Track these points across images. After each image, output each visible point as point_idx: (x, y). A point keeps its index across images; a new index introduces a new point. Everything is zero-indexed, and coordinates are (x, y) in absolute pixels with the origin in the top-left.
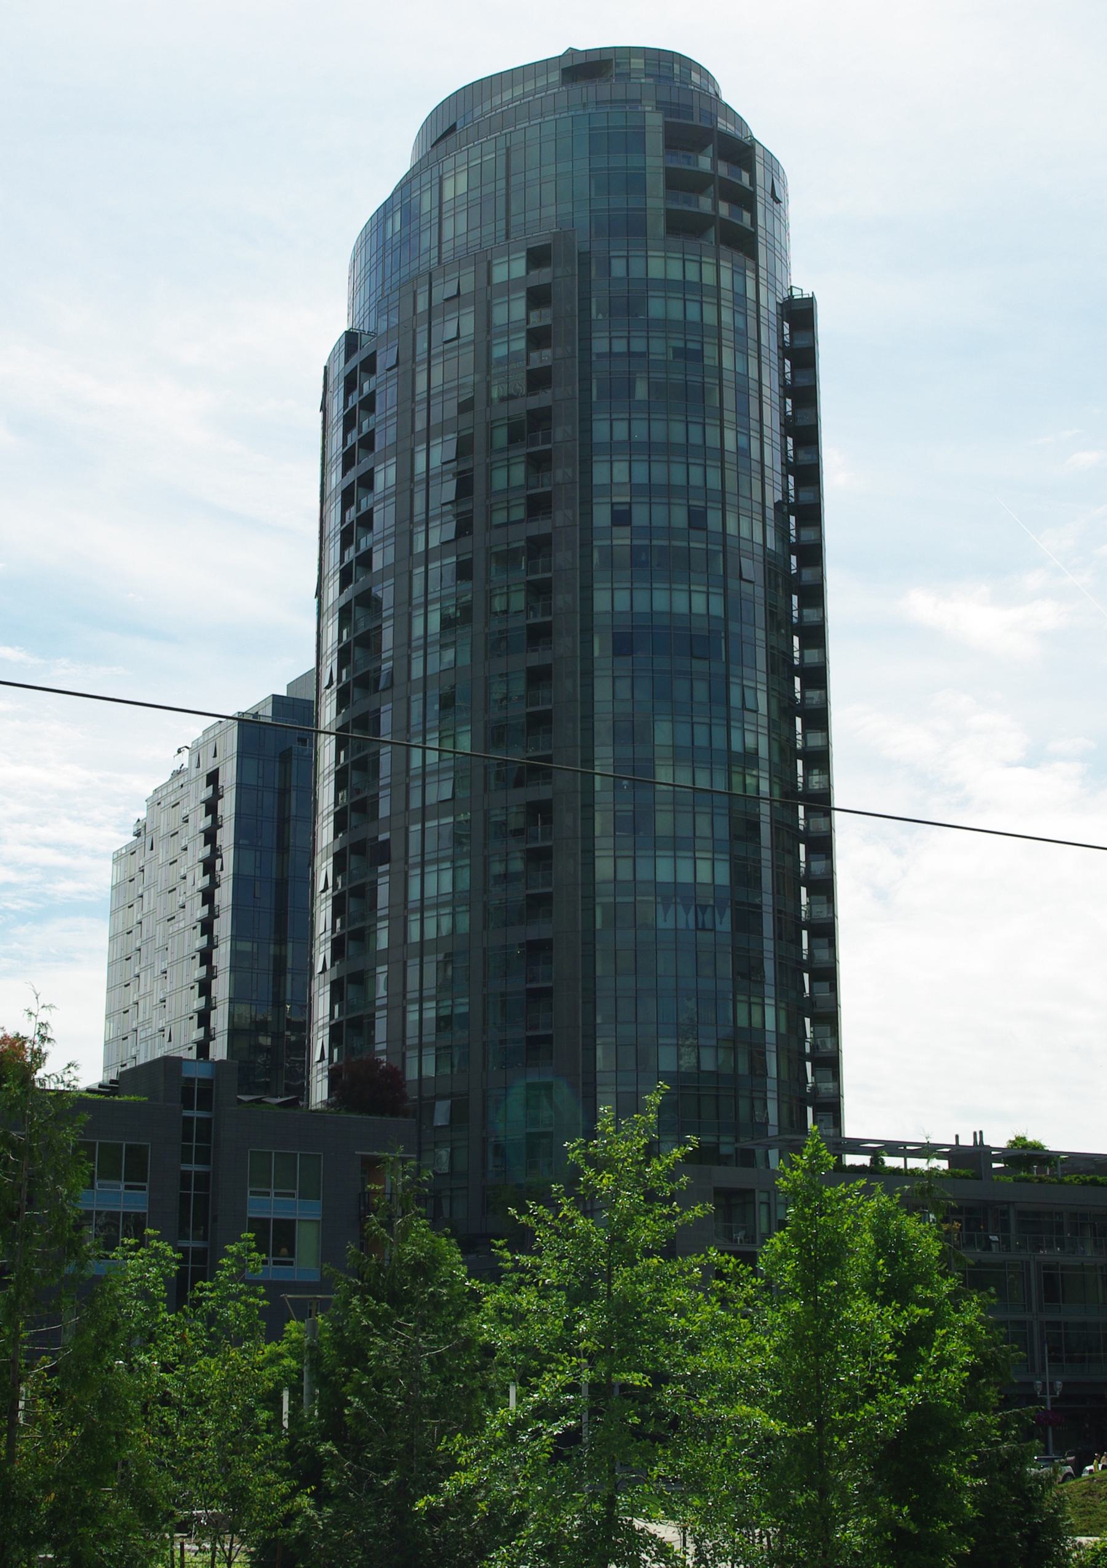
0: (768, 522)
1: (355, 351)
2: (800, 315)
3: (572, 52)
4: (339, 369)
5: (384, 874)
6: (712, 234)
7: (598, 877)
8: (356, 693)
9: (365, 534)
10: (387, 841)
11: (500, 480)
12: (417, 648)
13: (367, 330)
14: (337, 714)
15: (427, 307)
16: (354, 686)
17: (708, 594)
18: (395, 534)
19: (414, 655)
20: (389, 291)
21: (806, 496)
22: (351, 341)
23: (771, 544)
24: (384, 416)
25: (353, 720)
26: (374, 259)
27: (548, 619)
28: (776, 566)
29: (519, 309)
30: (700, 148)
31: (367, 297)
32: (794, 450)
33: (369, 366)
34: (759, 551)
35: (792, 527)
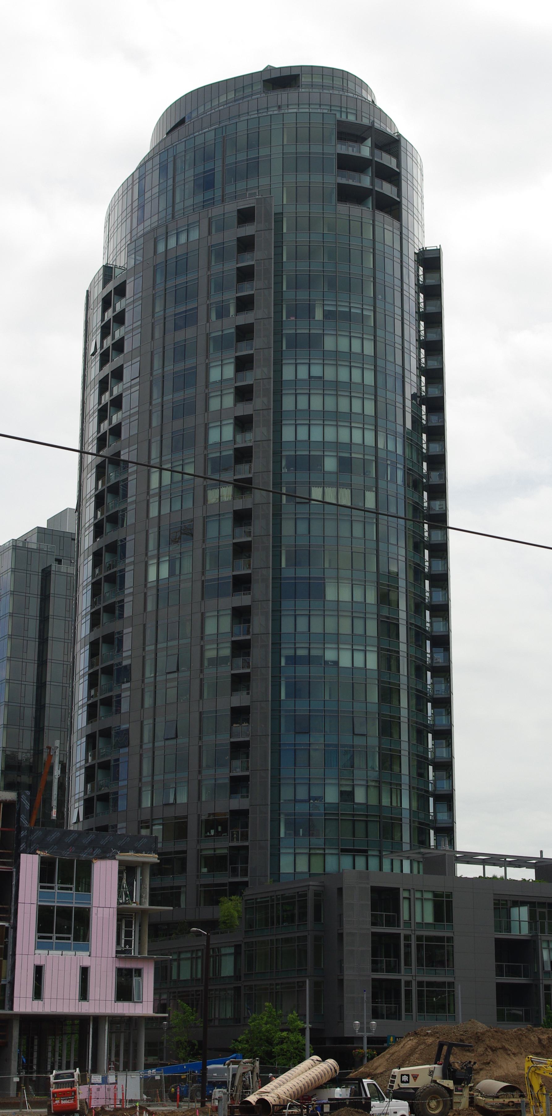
0: (407, 409)
1: (110, 280)
2: (431, 261)
3: (269, 69)
4: (99, 292)
5: (126, 689)
6: (370, 202)
7: (283, 630)
8: (107, 527)
9: (116, 412)
10: (127, 730)
11: (215, 375)
12: (154, 495)
13: (118, 265)
14: (94, 542)
15: (160, 423)
16: (108, 492)
17: (363, 429)
18: (142, 298)
19: (151, 500)
20: (135, 238)
21: (434, 392)
22: (108, 272)
23: (409, 425)
24: (131, 327)
25: (105, 546)
26: (124, 214)
27: (248, 637)
28: (411, 440)
29: (229, 400)
30: (360, 139)
31: (119, 241)
32: (426, 386)
33: (120, 291)
34: (400, 429)
35: (423, 413)
